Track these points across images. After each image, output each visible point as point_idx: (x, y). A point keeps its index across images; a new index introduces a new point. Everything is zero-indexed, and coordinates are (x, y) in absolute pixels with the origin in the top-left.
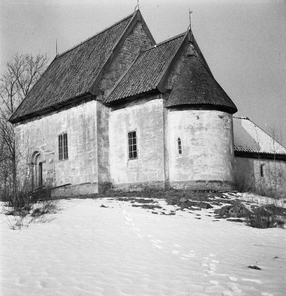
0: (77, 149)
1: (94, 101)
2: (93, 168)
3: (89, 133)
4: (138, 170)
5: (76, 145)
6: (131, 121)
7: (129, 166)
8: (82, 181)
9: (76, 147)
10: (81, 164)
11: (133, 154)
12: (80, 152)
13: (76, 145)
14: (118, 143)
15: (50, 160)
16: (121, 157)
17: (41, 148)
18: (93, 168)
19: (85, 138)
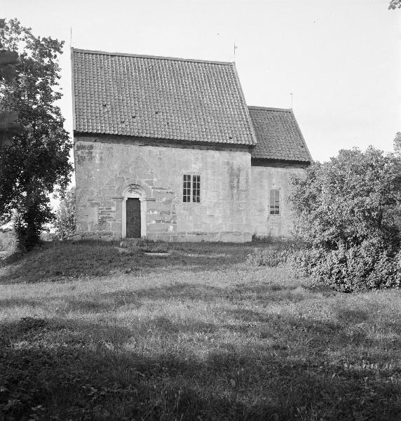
0: (218, 196)
5: (217, 191)
6: (274, 181)
10: (225, 212)
11: (275, 211)
12: (224, 199)
13: (217, 191)
15: (164, 199)
16: (261, 210)
17: (147, 182)
19: (232, 188)
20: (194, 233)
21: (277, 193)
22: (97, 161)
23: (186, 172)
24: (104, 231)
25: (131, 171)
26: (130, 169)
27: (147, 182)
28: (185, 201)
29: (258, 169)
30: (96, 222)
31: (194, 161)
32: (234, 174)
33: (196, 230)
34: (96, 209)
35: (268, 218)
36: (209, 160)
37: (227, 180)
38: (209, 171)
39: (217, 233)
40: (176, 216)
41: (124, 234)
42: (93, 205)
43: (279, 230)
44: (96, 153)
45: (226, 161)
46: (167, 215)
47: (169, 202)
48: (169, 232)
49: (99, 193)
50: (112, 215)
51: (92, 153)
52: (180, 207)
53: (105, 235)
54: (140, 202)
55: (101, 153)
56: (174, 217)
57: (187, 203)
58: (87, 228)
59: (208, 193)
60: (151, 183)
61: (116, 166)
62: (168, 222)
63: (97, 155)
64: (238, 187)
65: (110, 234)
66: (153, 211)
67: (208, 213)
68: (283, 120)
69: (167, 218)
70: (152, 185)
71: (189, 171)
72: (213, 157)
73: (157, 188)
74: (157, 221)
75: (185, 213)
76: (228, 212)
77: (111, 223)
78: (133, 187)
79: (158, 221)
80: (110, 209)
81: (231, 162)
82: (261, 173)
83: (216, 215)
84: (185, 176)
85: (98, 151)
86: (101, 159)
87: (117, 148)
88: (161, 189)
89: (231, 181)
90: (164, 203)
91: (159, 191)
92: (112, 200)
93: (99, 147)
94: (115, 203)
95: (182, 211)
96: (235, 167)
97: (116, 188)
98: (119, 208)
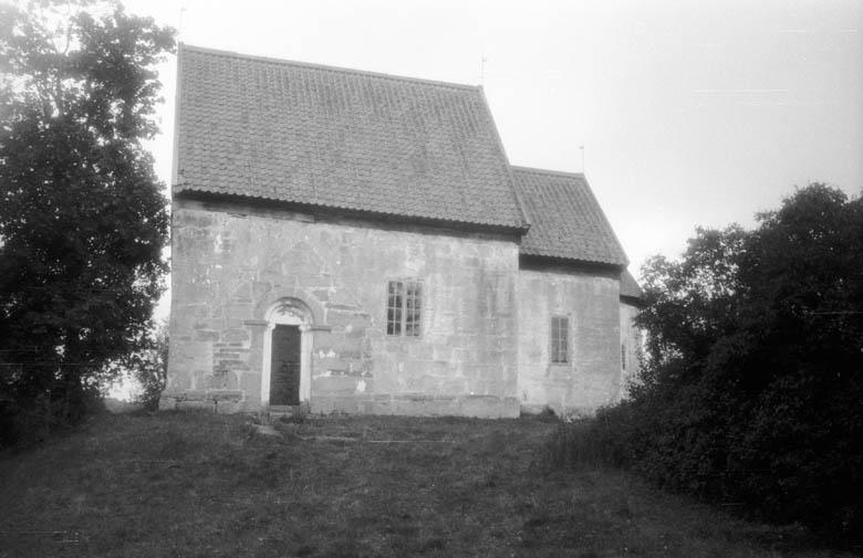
0: (455, 323)
1: (512, 244)
2: (505, 369)
3: (494, 297)
4: (569, 385)
6: (559, 299)
7: (551, 376)
8: (469, 389)
9: (451, 319)
11: (560, 355)
14: (534, 331)
15: (349, 328)
16: (535, 355)
17: (315, 293)
18: (505, 369)
19: (482, 309)
20: (406, 397)
21: (564, 322)
22: (218, 249)
23: (391, 275)
24: (224, 389)
25: (285, 273)
26: (283, 266)
27: (315, 293)
28: (390, 331)
29: (531, 276)
30: (211, 372)
31: (409, 255)
32: (485, 283)
33: (410, 392)
34: (210, 344)
35: (548, 371)
36: (439, 254)
37: (474, 294)
38: (438, 276)
39: (455, 398)
40: (370, 362)
41: (265, 396)
42: (205, 337)
43: (569, 394)
44: (217, 234)
45: (472, 257)
46: (356, 358)
47: (358, 333)
48: (356, 393)
49: (218, 312)
50: (244, 357)
51: (206, 232)
52: (381, 346)
53: (226, 398)
54: (299, 332)
55: (227, 234)
56: (369, 365)
57: (393, 338)
58: (189, 383)
59: (436, 323)
60: (323, 296)
61: (255, 261)
62: (357, 374)
63: (219, 238)
64: (494, 308)
65: (238, 396)
66: (326, 350)
67: (435, 356)
68: (571, 194)
69: (352, 367)
70: (327, 299)
71: (397, 274)
72: (447, 249)
73: (336, 307)
74: (333, 371)
75: (391, 356)
76: (474, 355)
77: (239, 373)
78: (288, 302)
79: (335, 372)
80: (238, 345)
81: (481, 259)
82: (534, 284)
83: (452, 361)
84: (391, 284)
85: (220, 228)
86: (226, 245)
87: (257, 224)
88: (342, 307)
89: (481, 297)
90: (349, 335)
91: (339, 311)
92: (244, 327)
93: (224, 223)
94: (250, 333)
95: (384, 352)
96: (489, 269)
97: (254, 303)
98: (257, 344)
